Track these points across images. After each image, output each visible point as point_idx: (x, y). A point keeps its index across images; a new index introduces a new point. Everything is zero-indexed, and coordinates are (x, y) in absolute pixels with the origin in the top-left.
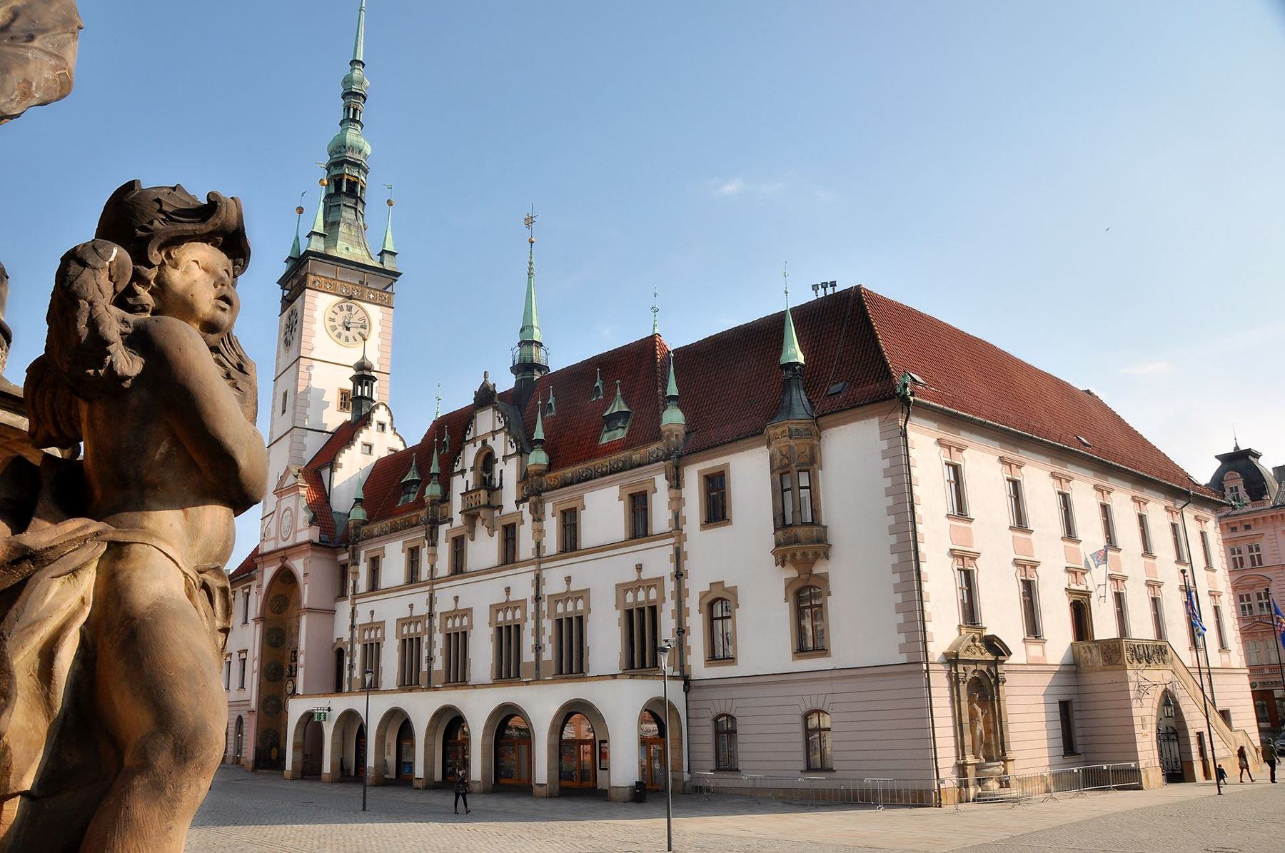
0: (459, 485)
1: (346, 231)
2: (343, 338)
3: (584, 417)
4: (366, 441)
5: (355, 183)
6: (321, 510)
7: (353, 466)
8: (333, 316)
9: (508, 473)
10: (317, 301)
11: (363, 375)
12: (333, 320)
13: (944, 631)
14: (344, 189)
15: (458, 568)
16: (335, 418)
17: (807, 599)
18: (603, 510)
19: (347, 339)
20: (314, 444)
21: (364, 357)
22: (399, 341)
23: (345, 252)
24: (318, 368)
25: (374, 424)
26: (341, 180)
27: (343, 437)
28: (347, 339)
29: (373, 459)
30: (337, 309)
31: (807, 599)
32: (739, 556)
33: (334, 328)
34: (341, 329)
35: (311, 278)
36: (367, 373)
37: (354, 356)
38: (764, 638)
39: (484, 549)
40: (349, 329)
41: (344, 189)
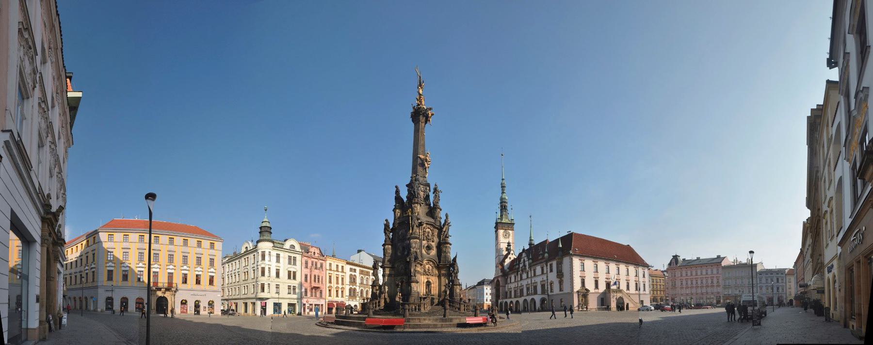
0: (521, 265)
3: (538, 253)
6: (503, 270)
7: (508, 261)
9: (527, 263)
11: (509, 244)
13: (577, 286)
15: (521, 279)
16: (505, 253)
17: (561, 283)
18: (538, 269)
20: (502, 258)
22: (514, 238)
27: (506, 257)
31: (561, 283)
32: (553, 277)
38: (556, 290)
39: (524, 276)
40: (506, 236)
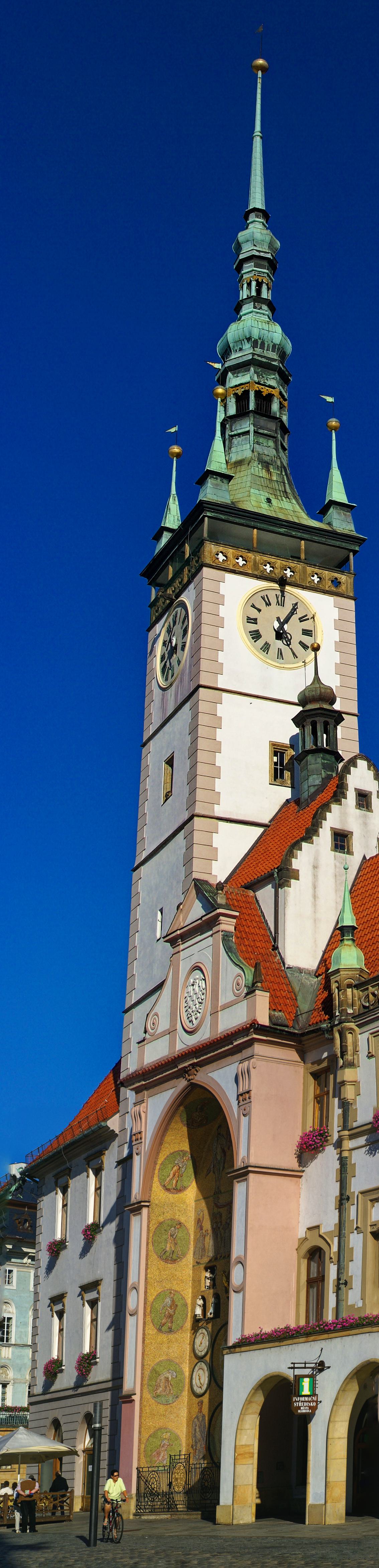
1: (264, 473)
2: (273, 651)
4: (338, 826)
5: (270, 397)
8: (254, 614)
10: (223, 589)
12: (255, 621)
14: (252, 406)
19: (280, 654)
21: (317, 678)
23: (265, 505)
24: (228, 707)
25: (351, 796)
26: (246, 393)
28: (280, 654)
29: (354, 862)
30: (261, 604)
33: (256, 635)
34: (269, 636)
35: (210, 548)
36: (326, 706)
37: (293, 681)
40: (283, 638)
41: (252, 406)
